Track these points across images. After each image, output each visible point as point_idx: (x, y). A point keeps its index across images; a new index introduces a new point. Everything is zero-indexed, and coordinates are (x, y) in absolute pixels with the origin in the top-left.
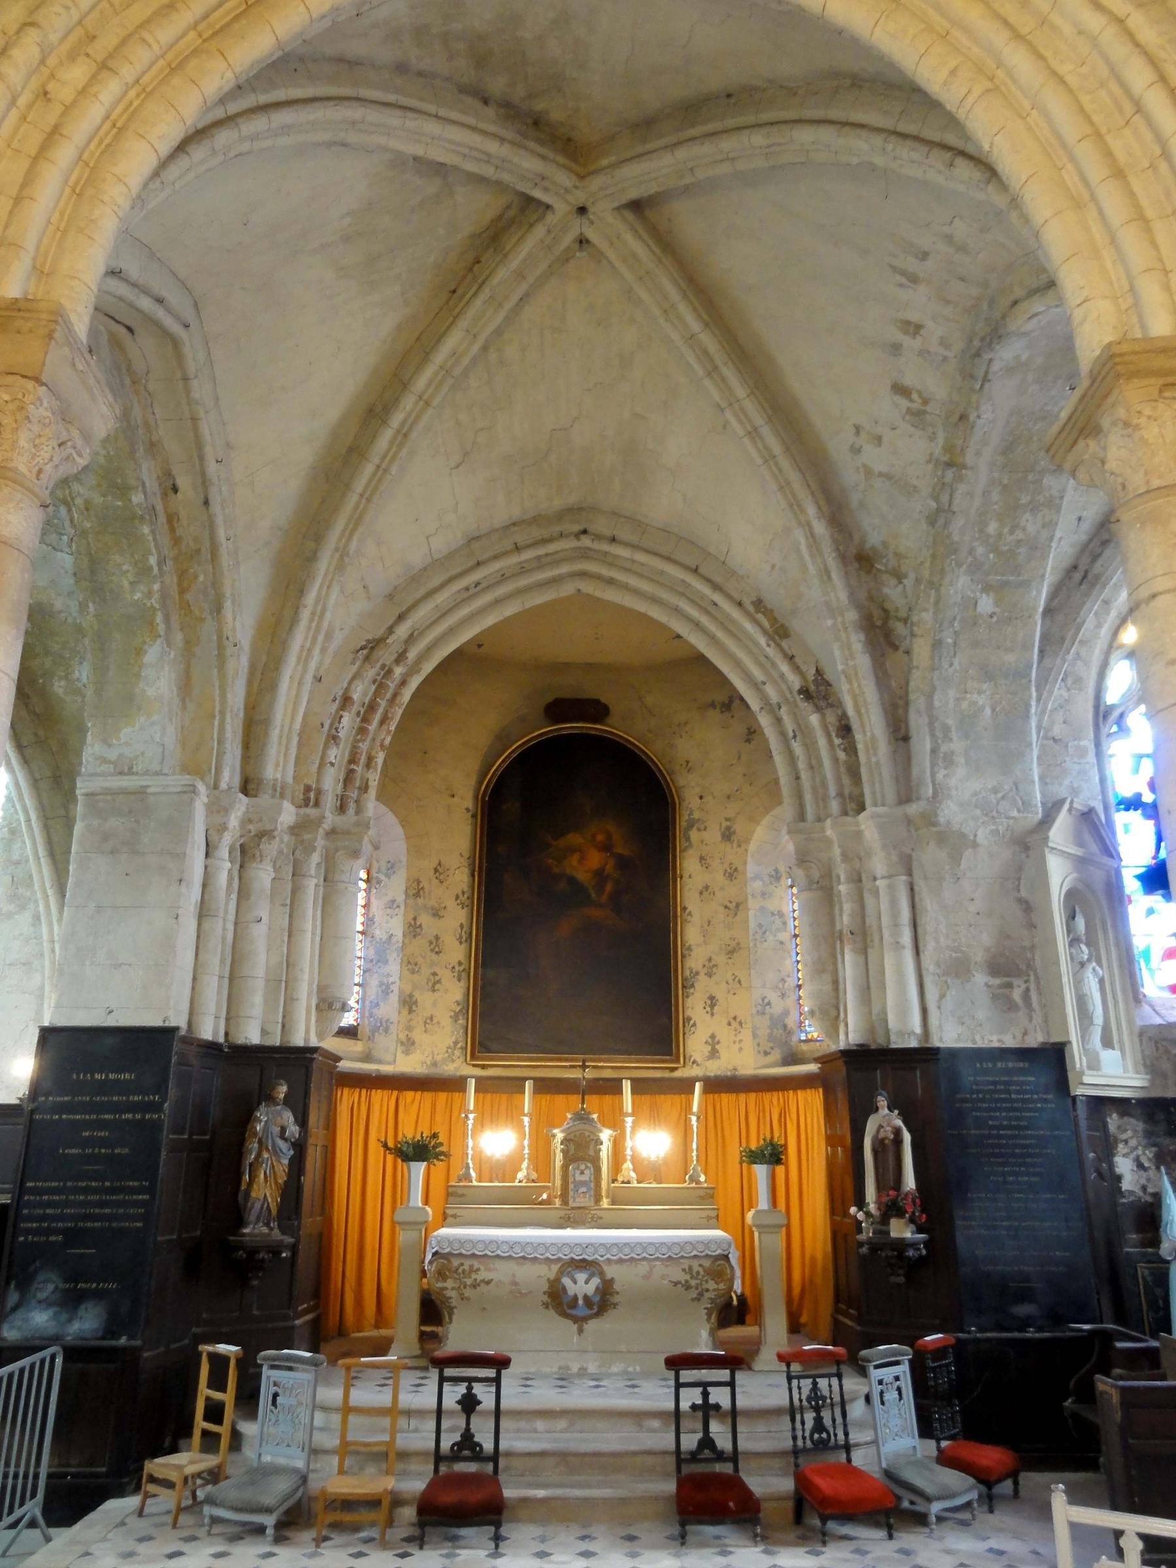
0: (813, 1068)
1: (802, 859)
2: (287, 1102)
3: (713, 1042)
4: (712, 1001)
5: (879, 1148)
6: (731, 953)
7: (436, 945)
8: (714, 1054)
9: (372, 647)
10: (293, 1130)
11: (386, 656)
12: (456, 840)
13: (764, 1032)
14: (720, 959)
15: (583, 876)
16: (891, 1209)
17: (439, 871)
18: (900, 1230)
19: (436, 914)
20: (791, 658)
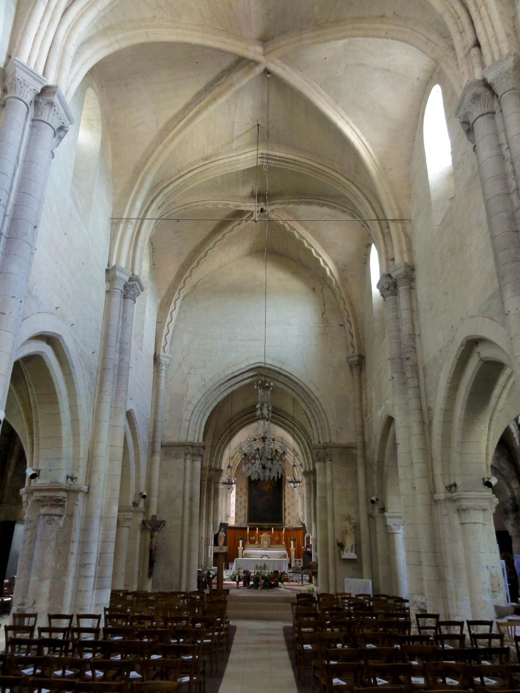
0: (302, 526)
1: (300, 494)
2: (223, 531)
3: (289, 521)
4: (289, 513)
5: (307, 538)
6: (292, 504)
7: (241, 503)
8: (289, 523)
9: (233, 457)
10: (224, 535)
11: (234, 459)
12: (244, 483)
13: (298, 519)
14: (290, 505)
15: (266, 490)
16: (307, 547)
17: (241, 489)
18: (308, 550)
19: (241, 497)
20: (298, 459)
